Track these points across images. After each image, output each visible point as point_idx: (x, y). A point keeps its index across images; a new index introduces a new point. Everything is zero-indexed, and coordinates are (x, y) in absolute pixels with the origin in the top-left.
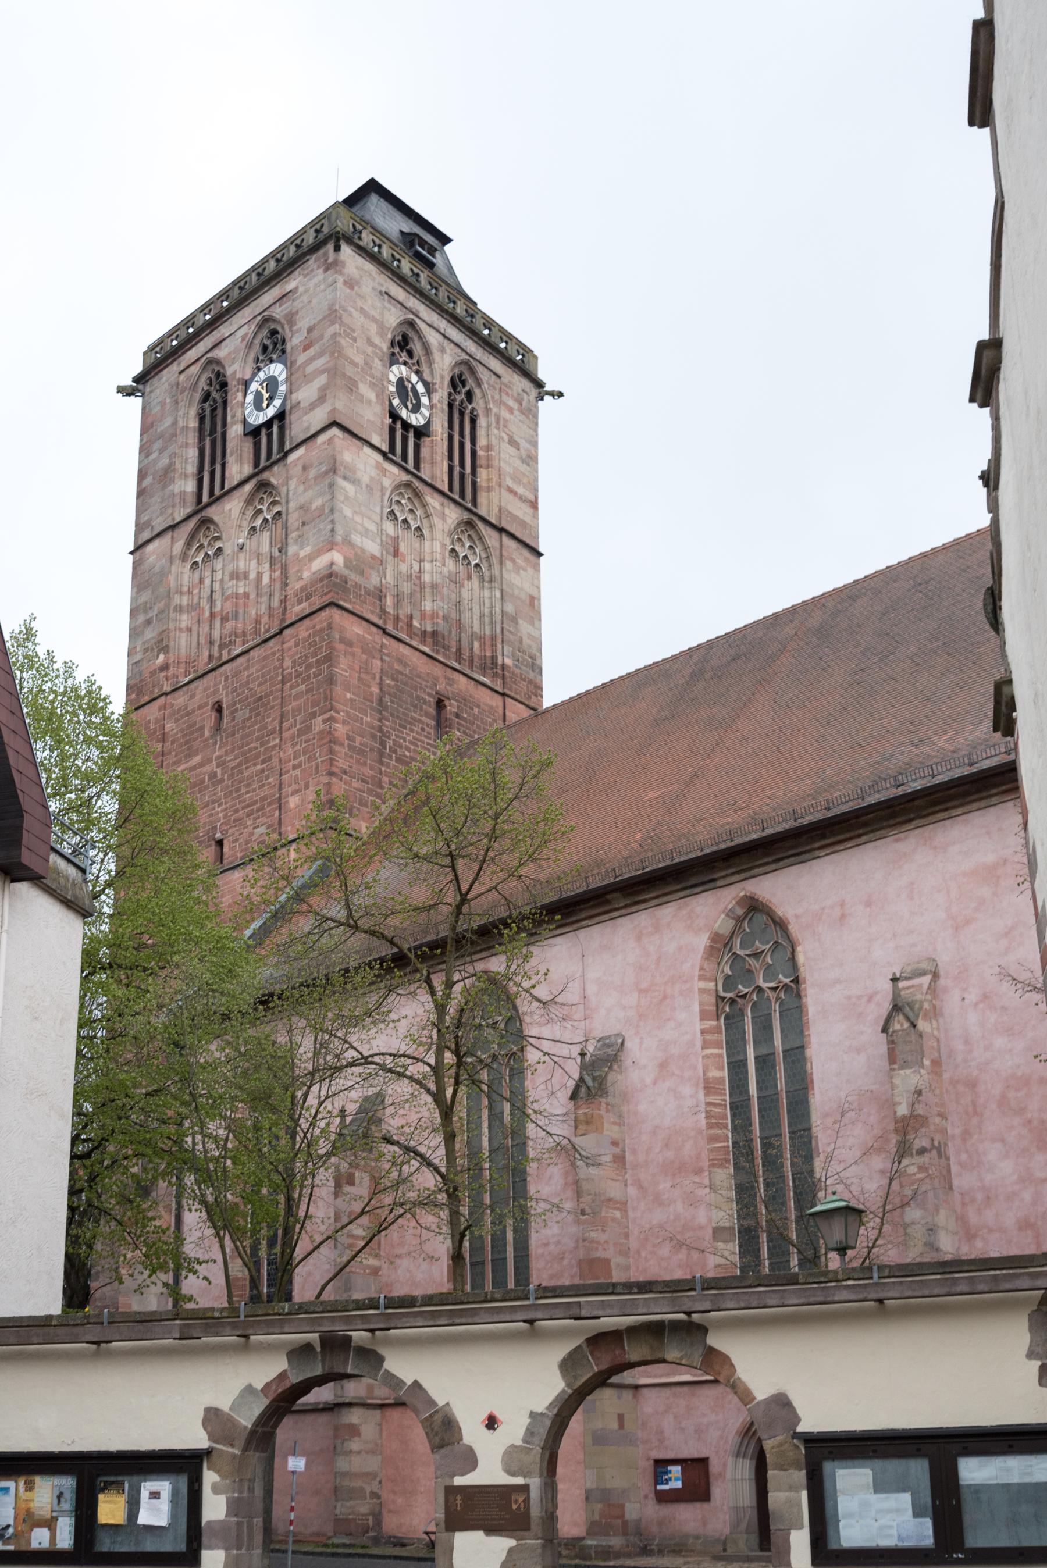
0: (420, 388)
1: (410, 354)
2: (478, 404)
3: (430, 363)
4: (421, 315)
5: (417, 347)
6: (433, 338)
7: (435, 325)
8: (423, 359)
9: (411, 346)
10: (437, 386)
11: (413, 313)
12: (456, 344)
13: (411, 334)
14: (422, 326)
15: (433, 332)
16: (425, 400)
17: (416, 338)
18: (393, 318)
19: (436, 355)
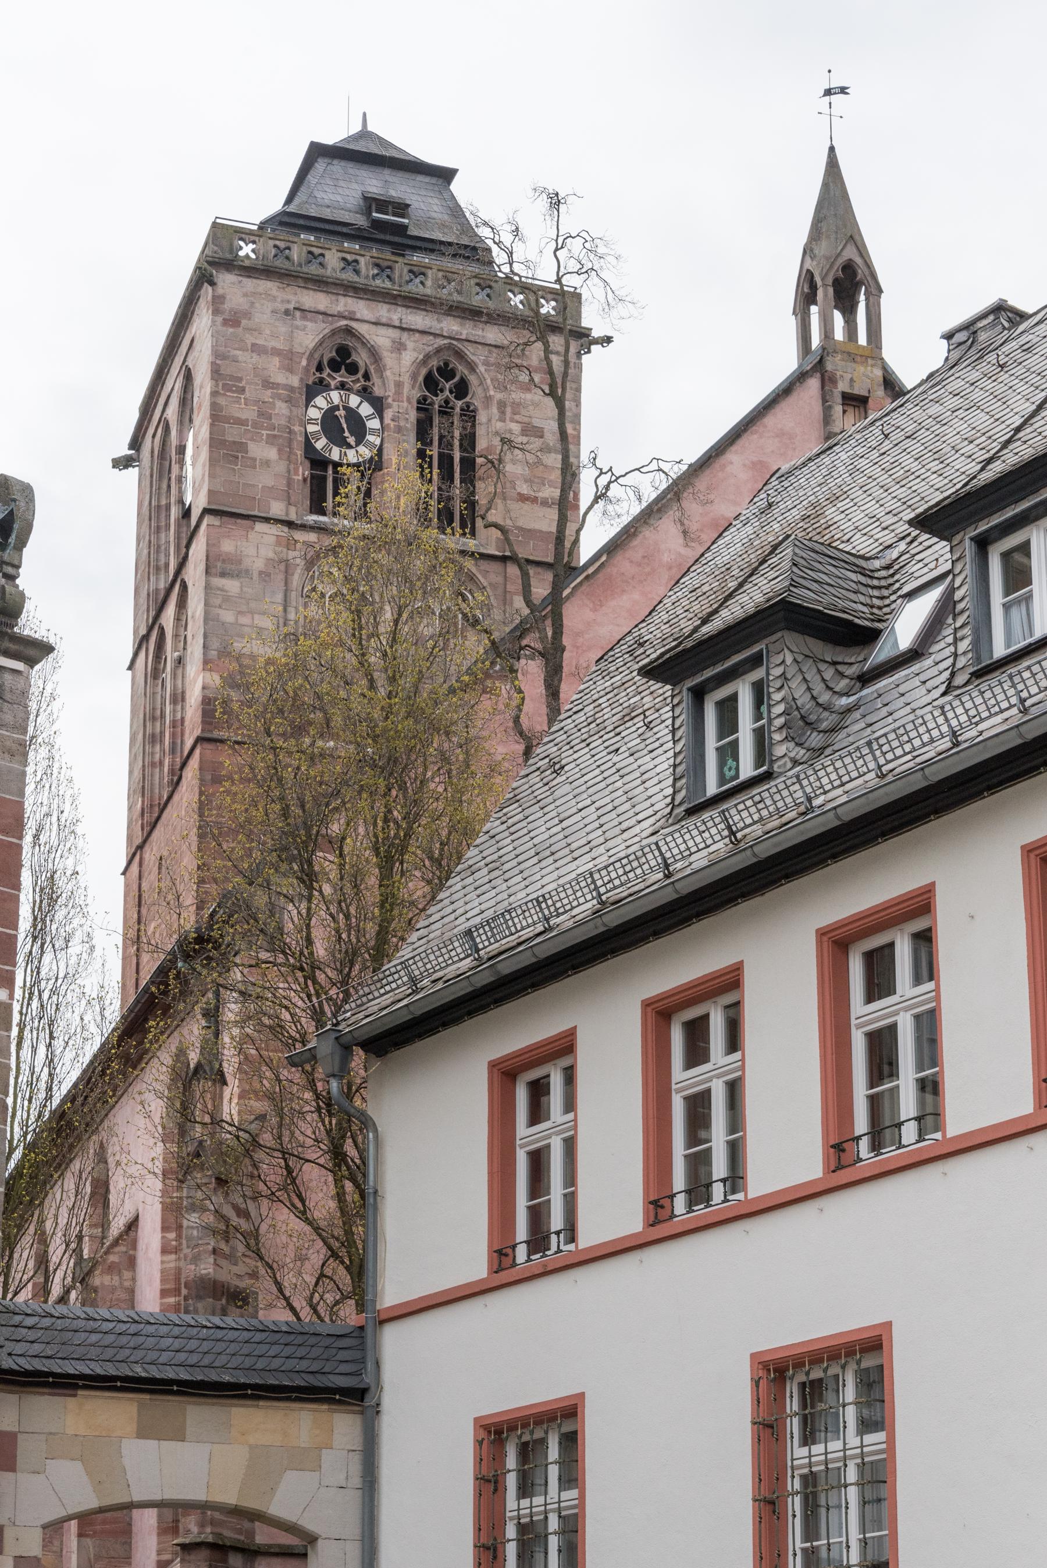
0: (366, 410)
1: (353, 369)
2: (476, 397)
3: (381, 371)
4: (358, 316)
5: (361, 358)
6: (381, 339)
7: (384, 320)
8: (372, 369)
9: (354, 357)
10: (390, 400)
11: (344, 318)
12: (423, 332)
13: (350, 342)
14: (362, 329)
15: (382, 331)
16: (374, 424)
17: (358, 345)
18: (309, 336)
19: (389, 359)
